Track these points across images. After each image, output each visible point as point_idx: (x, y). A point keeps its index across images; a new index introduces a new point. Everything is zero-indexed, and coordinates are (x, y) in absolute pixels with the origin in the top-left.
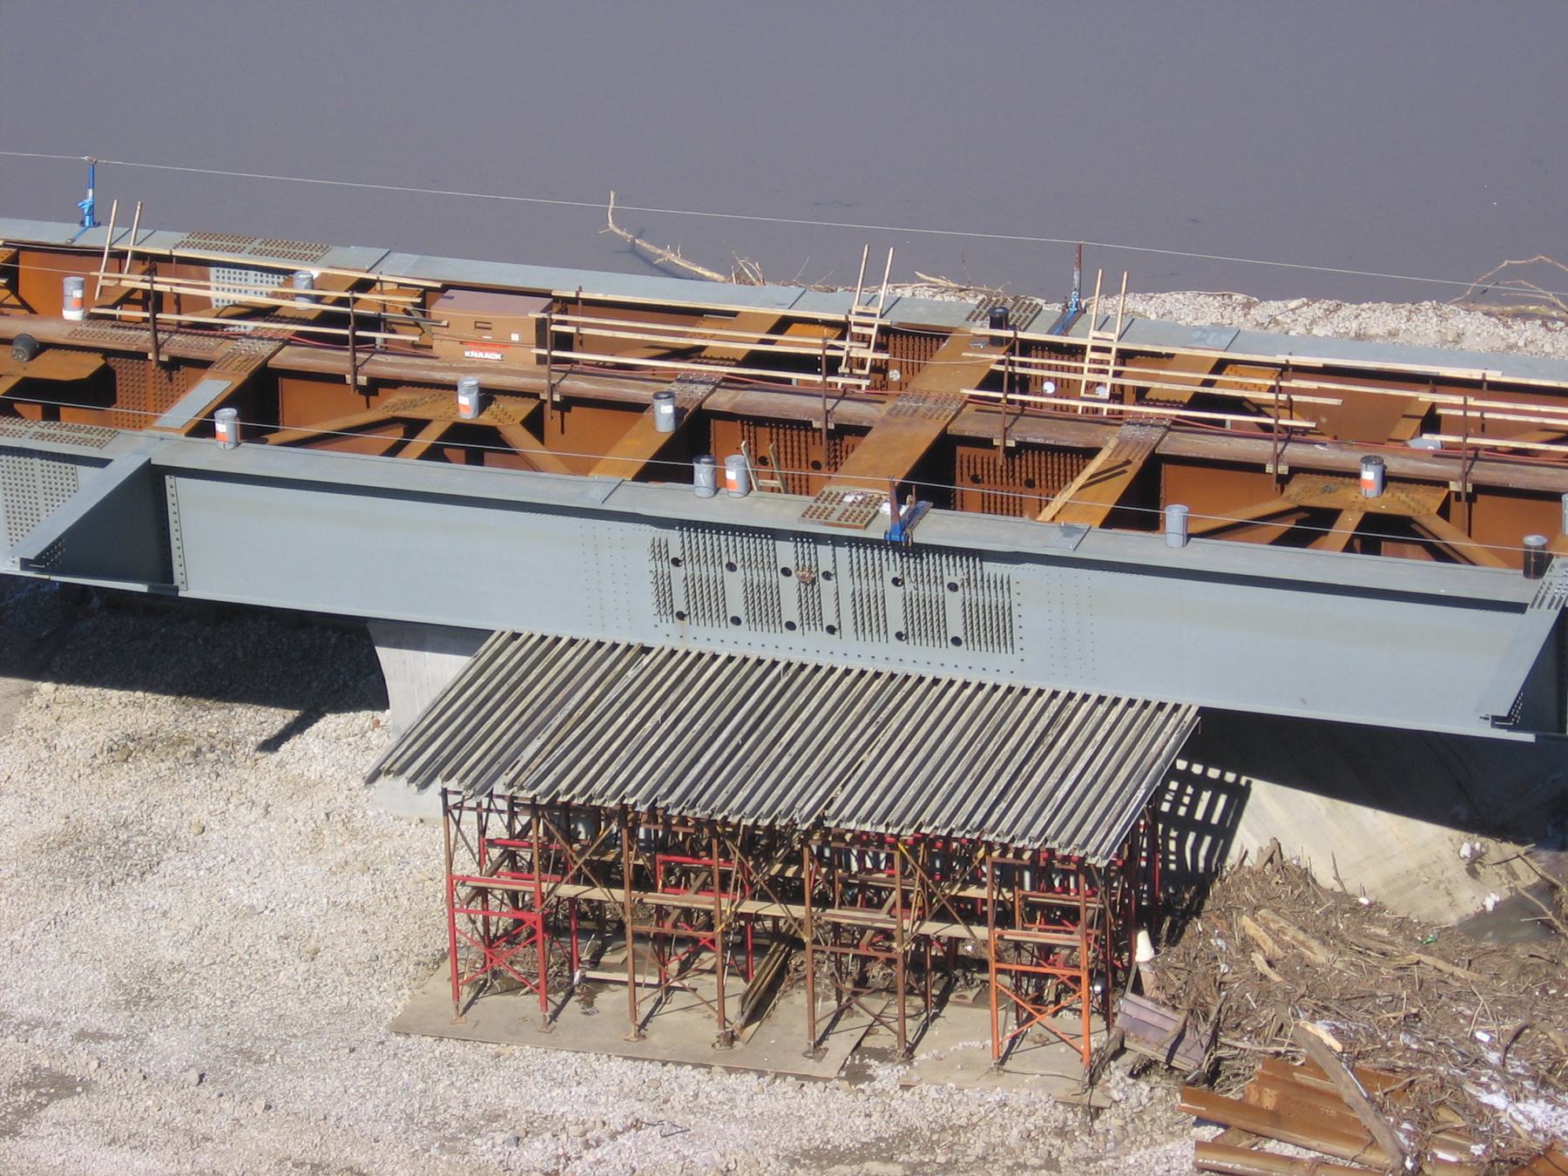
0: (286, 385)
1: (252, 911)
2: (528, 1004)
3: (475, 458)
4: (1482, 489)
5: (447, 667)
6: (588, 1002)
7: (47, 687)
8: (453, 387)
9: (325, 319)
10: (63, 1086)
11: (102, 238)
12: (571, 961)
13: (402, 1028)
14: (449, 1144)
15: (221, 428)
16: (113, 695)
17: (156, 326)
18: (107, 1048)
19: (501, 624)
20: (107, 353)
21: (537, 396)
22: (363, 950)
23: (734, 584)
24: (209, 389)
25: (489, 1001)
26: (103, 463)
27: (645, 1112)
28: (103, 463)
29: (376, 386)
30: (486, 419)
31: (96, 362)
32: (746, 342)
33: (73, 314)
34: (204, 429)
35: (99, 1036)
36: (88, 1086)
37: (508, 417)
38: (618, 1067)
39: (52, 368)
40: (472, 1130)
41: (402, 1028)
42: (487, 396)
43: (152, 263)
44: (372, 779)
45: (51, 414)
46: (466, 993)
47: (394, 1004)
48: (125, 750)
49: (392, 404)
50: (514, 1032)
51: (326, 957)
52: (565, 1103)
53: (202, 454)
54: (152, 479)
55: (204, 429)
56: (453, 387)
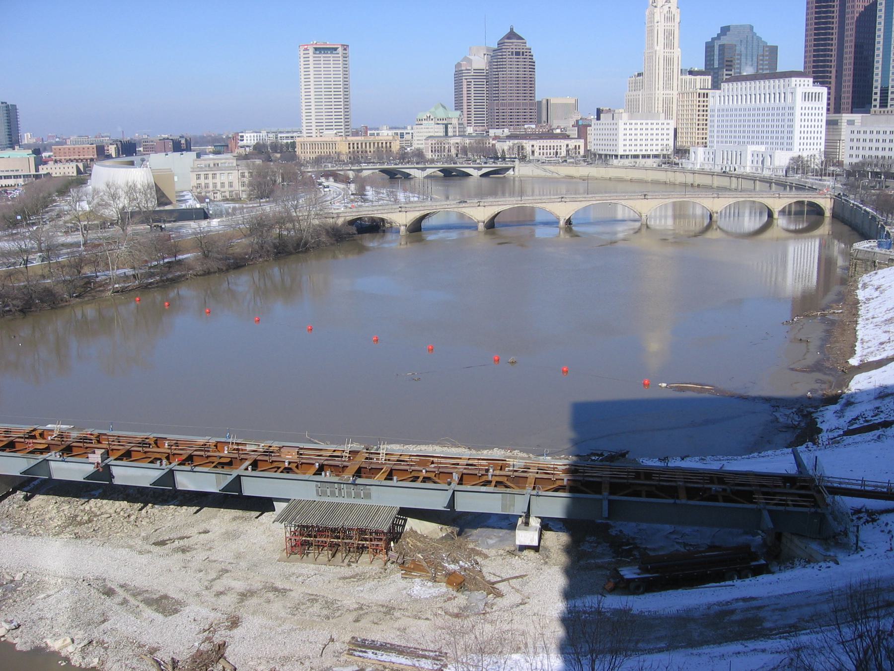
0: (259, 462)
1: (255, 543)
2: (298, 556)
3: (288, 473)
4: (440, 472)
5: (284, 505)
6: (307, 556)
7: (222, 509)
8: (284, 462)
9: (265, 452)
10: (227, 571)
11: (230, 440)
12: (305, 550)
13: (278, 561)
14: (287, 578)
15: (249, 469)
16: (233, 510)
17: (239, 454)
18: (233, 565)
19: (293, 498)
20: (231, 458)
21: (296, 463)
22: (272, 549)
23: (328, 491)
24: (247, 463)
25: (292, 556)
26: (231, 475)
27: (317, 572)
28: (231, 475)
29: (273, 462)
30: (290, 466)
31: (230, 459)
32: (329, 454)
33: (226, 452)
34: (247, 469)
35: (232, 563)
36: (231, 571)
37: (293, 466)
38: (312, 566)
39: (223, 460)
40: (291, 576)
41: (278, 561)
42: (289, 463)
43: (238, 444)
44: (273, 522)
45: (223, 467)
46: (289, 555)
47: (278, 557)
48: (234, 519)
49: (275, 464)
50: (296, 561)
51: (266, 550)
52: (304, 571)
53: (246, 473)
54: (239, 477)
55: (247, 469)
56: (284, 462)
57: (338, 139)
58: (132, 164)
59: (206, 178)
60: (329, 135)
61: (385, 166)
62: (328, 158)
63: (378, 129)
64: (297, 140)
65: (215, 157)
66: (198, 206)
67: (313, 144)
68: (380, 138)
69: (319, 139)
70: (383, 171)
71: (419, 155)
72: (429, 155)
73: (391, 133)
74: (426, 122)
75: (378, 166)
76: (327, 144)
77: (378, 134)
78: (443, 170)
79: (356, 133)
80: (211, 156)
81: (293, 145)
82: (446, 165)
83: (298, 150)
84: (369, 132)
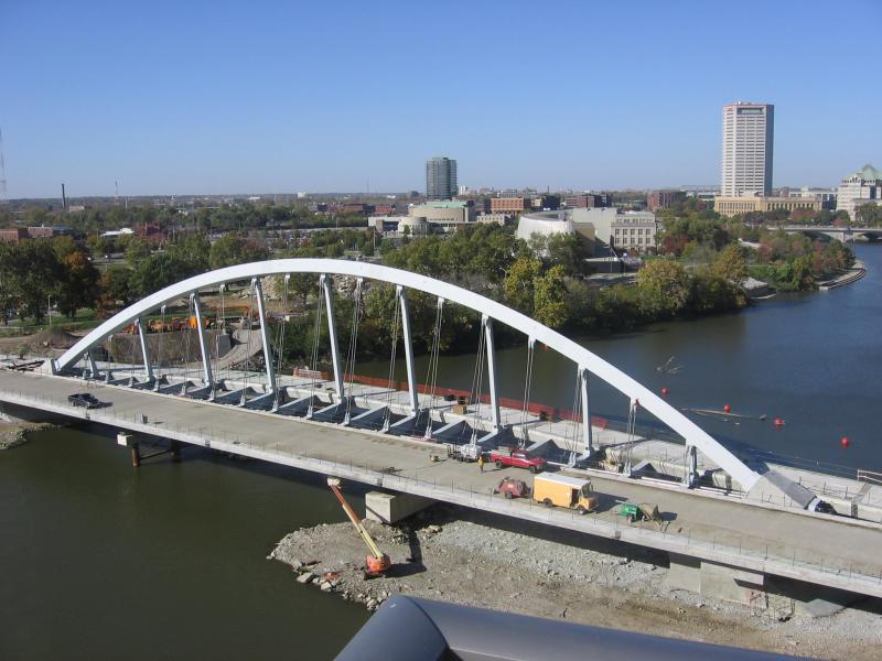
57: (758, 199)
58: (555, 217)
59: (625, 233)
60: (749, 196)
61: (806, 228)
62: (749, 217)
63: (799, 190)
64: (717, 199)
65: (636, 213)
66: (616, 259)
67: (731, 204)
68: (799, 199)
69: (739, 199)
70: (807, 233)
71: (844, 214)
72: (853, 218)
73: (813, 194)
74: (852, 184)
75: (798, 228)
76: (747, 204)
77: (800, 195)
78: (868, 234)
79: (778, 196)
80: (631, 212)
81: (712, 204)
82: (871, 229)
83: (716, 209)
84: (790, 193)
